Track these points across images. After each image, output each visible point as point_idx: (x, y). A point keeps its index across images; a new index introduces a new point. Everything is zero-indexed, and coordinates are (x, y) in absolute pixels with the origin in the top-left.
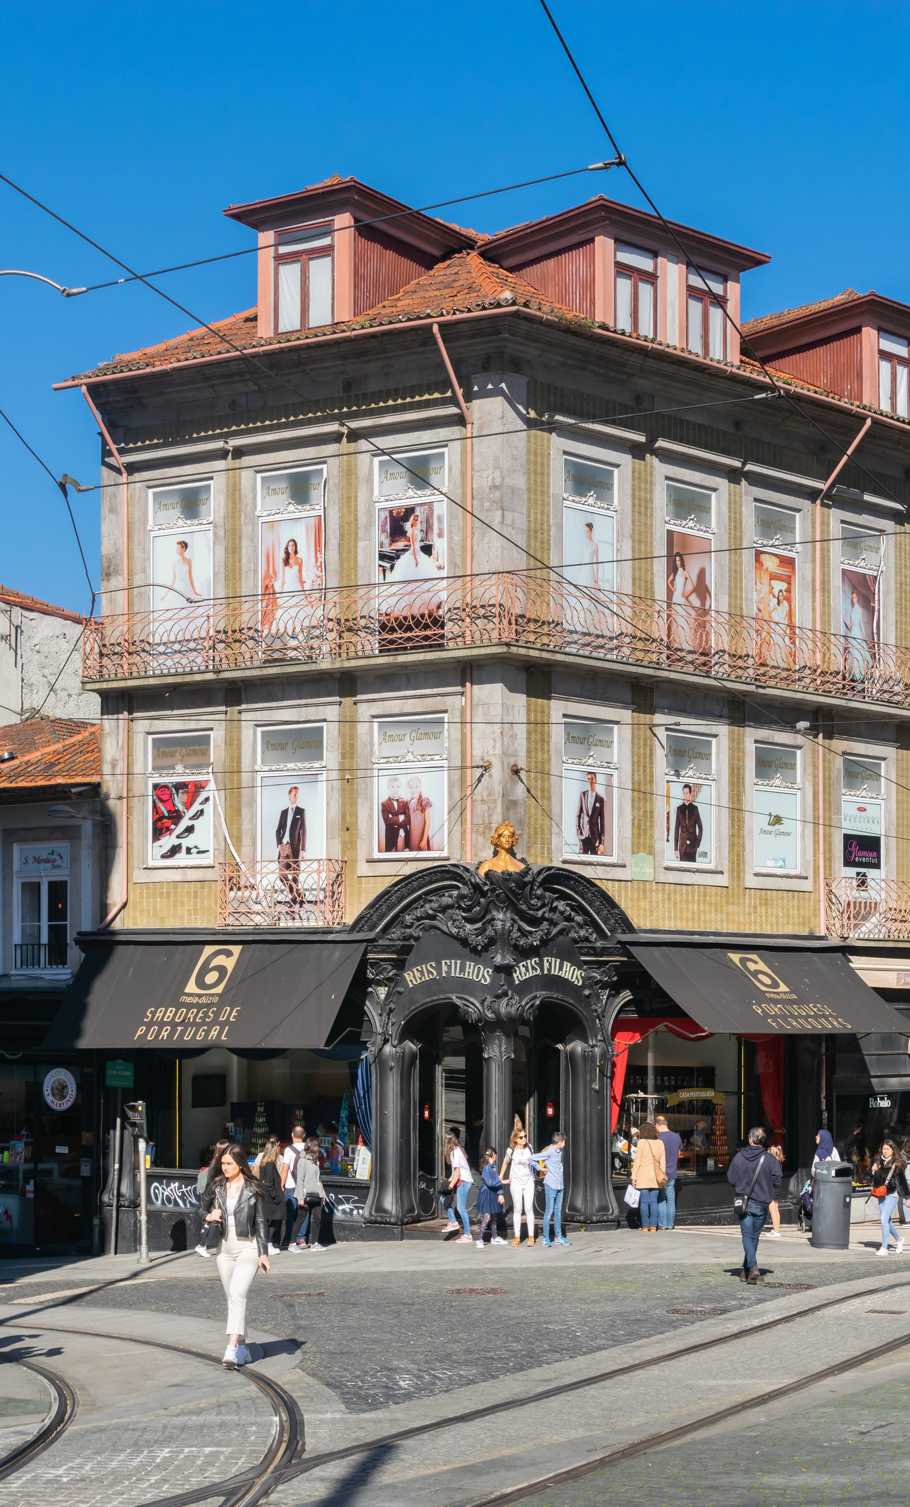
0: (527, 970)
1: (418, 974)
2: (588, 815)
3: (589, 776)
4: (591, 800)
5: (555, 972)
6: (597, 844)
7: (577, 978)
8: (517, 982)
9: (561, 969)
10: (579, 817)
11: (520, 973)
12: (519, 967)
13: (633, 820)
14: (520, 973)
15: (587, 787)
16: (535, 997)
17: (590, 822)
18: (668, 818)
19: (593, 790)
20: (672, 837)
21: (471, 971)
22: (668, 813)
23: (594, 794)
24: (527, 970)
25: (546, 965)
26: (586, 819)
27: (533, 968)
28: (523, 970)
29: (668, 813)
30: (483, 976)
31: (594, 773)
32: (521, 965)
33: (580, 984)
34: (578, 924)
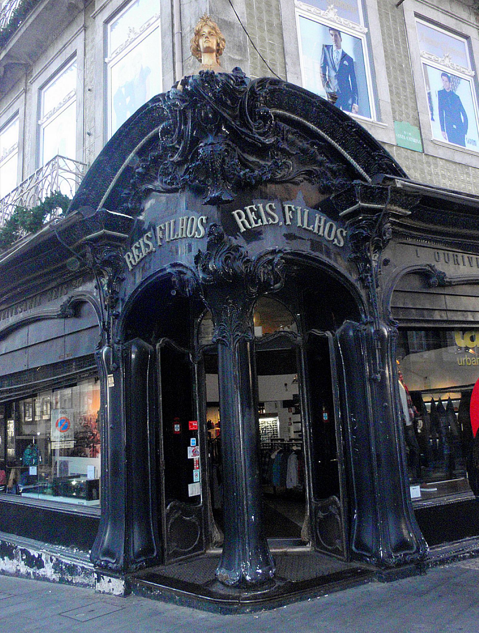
0: (259, 216)
1: (136, 252)
2: (334, 69)
3: (331, 32)
4: (336, 57)
5: (302, 221)
6: (350, 102)
7: (336, 236)
8: (243, 230)
9: (311, 221)
10: (324, 69)
11: (247, 218)
12: (245, 211)
13: (390, 86)
14: (247, 218)
15: (331, 41)
16: (273, 252)
17: (337, 77)
18: (430, 98)
19: (338, 47)
20: (437, 117)
21: (184, 227)
22: (429, 94)
23: (340, 51)
24: (259, 216)
25: (288, 214)
26: (333, 74)
27: (267, 214)
28: (252, 216)
29: (429, 94)
30: (197, 229)
31: (339, 32)
32: (247, 208)
33: (342, 244)
34: (331, 170)
